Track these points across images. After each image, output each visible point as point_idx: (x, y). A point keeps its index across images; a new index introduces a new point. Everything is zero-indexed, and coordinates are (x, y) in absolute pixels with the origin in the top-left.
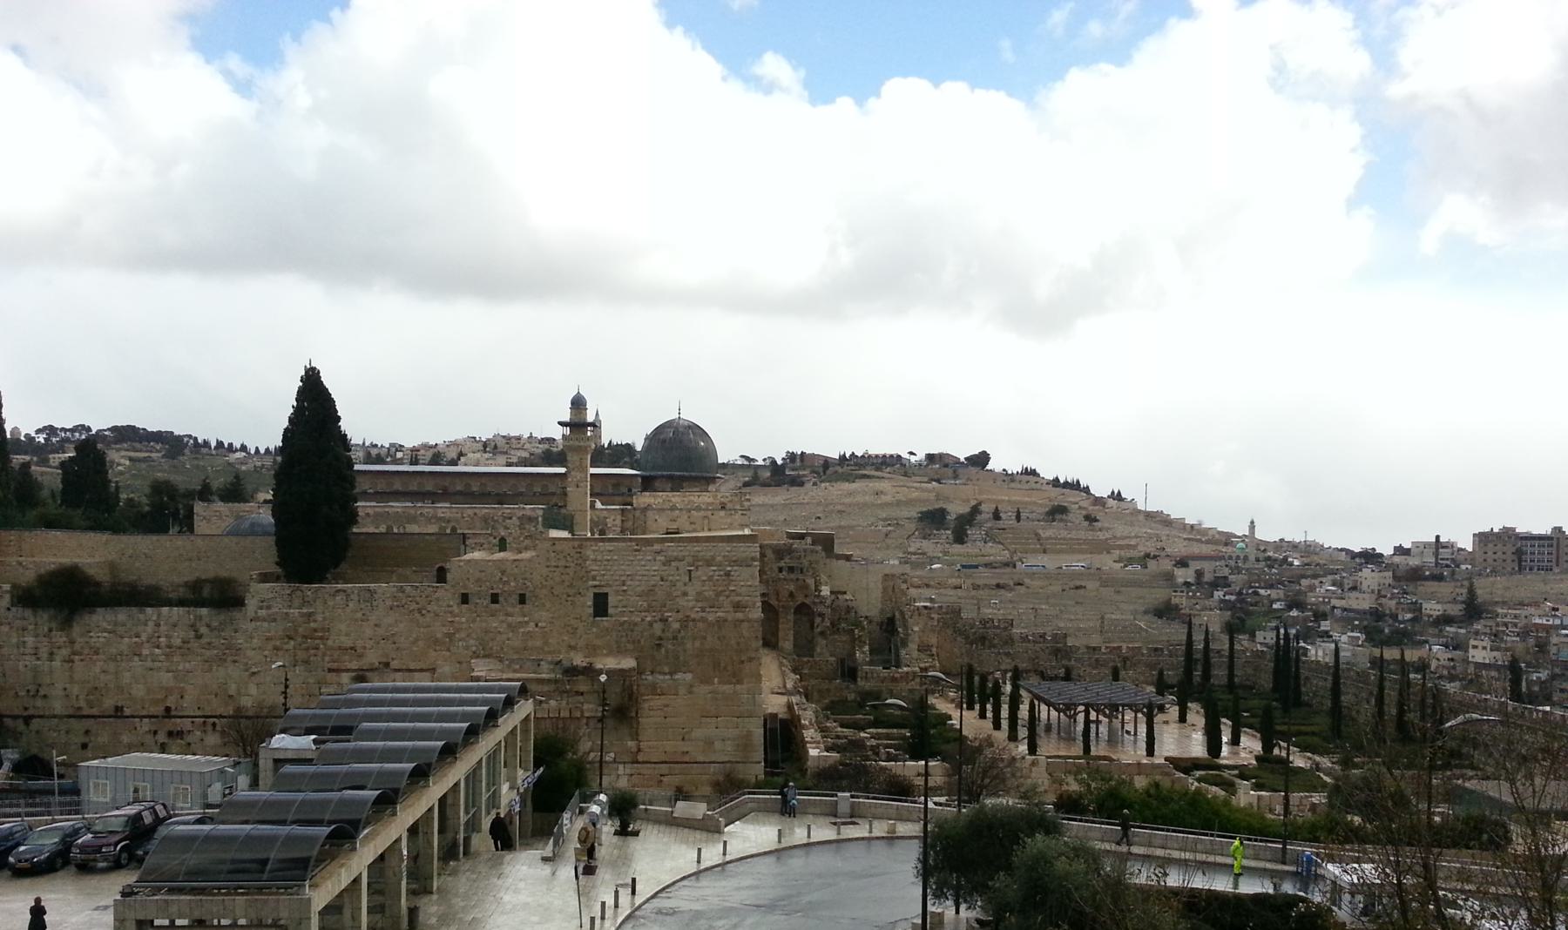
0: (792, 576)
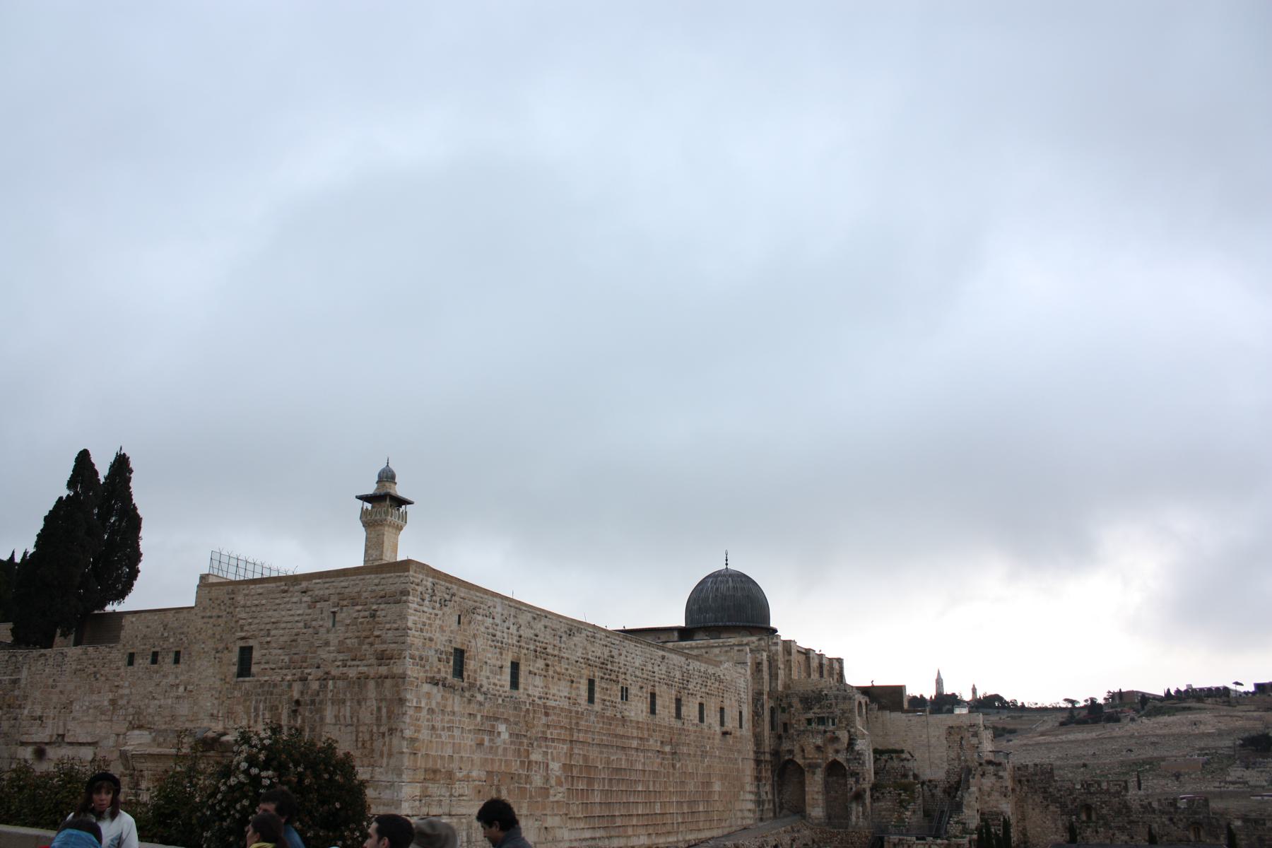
0: (821, 728)
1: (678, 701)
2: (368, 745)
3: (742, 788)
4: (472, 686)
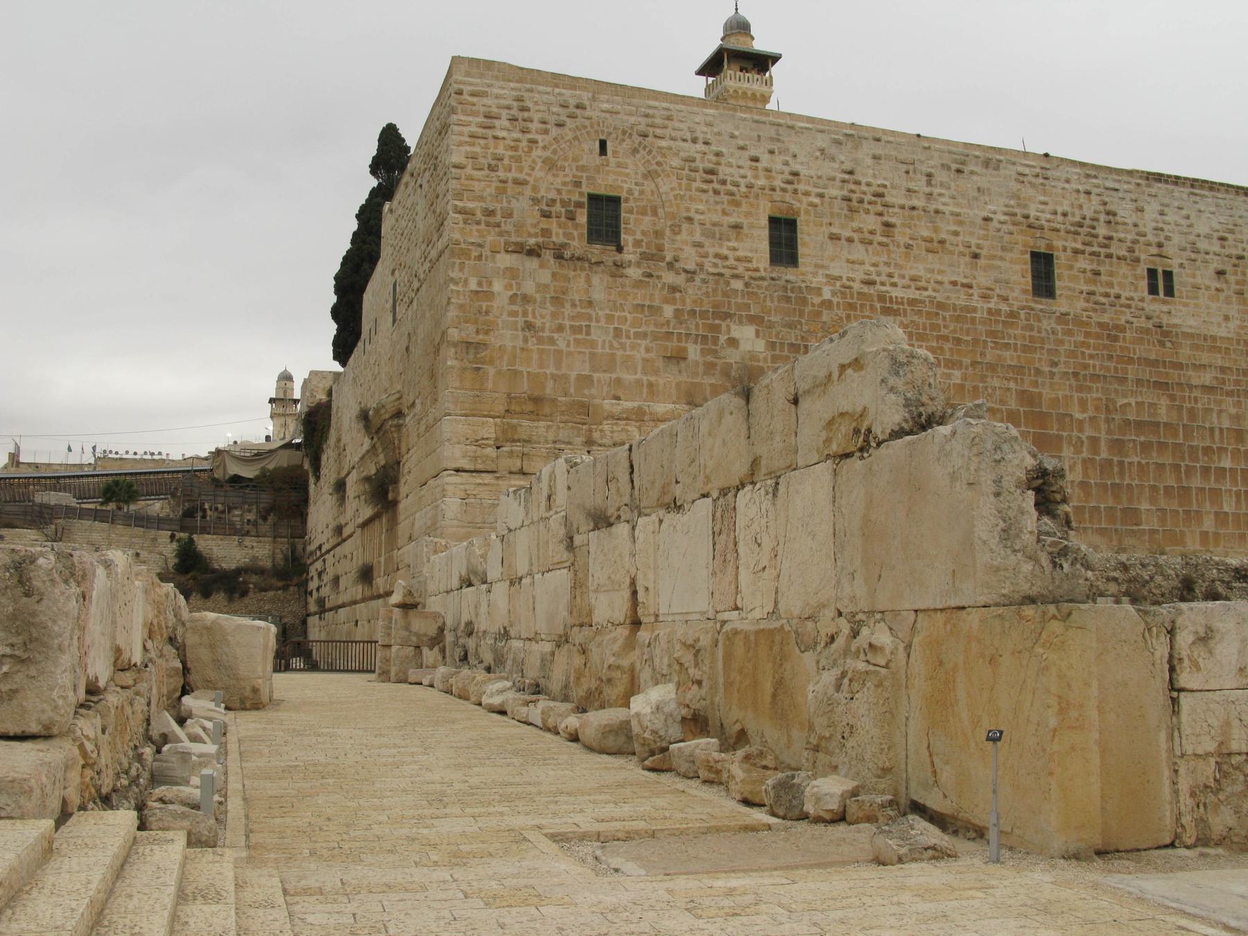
4: (652, 256)
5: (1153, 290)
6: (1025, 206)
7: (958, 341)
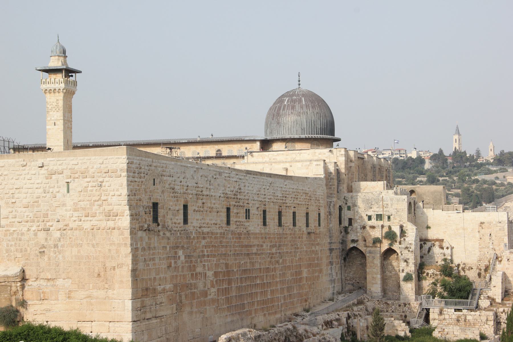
0: (380, 223)
1: (280, 213)
2: (102, 274)
3: (321, 271)
4: (164, 226)
5: (246, 219)
6: (225, 189)
7: (215, 246)
